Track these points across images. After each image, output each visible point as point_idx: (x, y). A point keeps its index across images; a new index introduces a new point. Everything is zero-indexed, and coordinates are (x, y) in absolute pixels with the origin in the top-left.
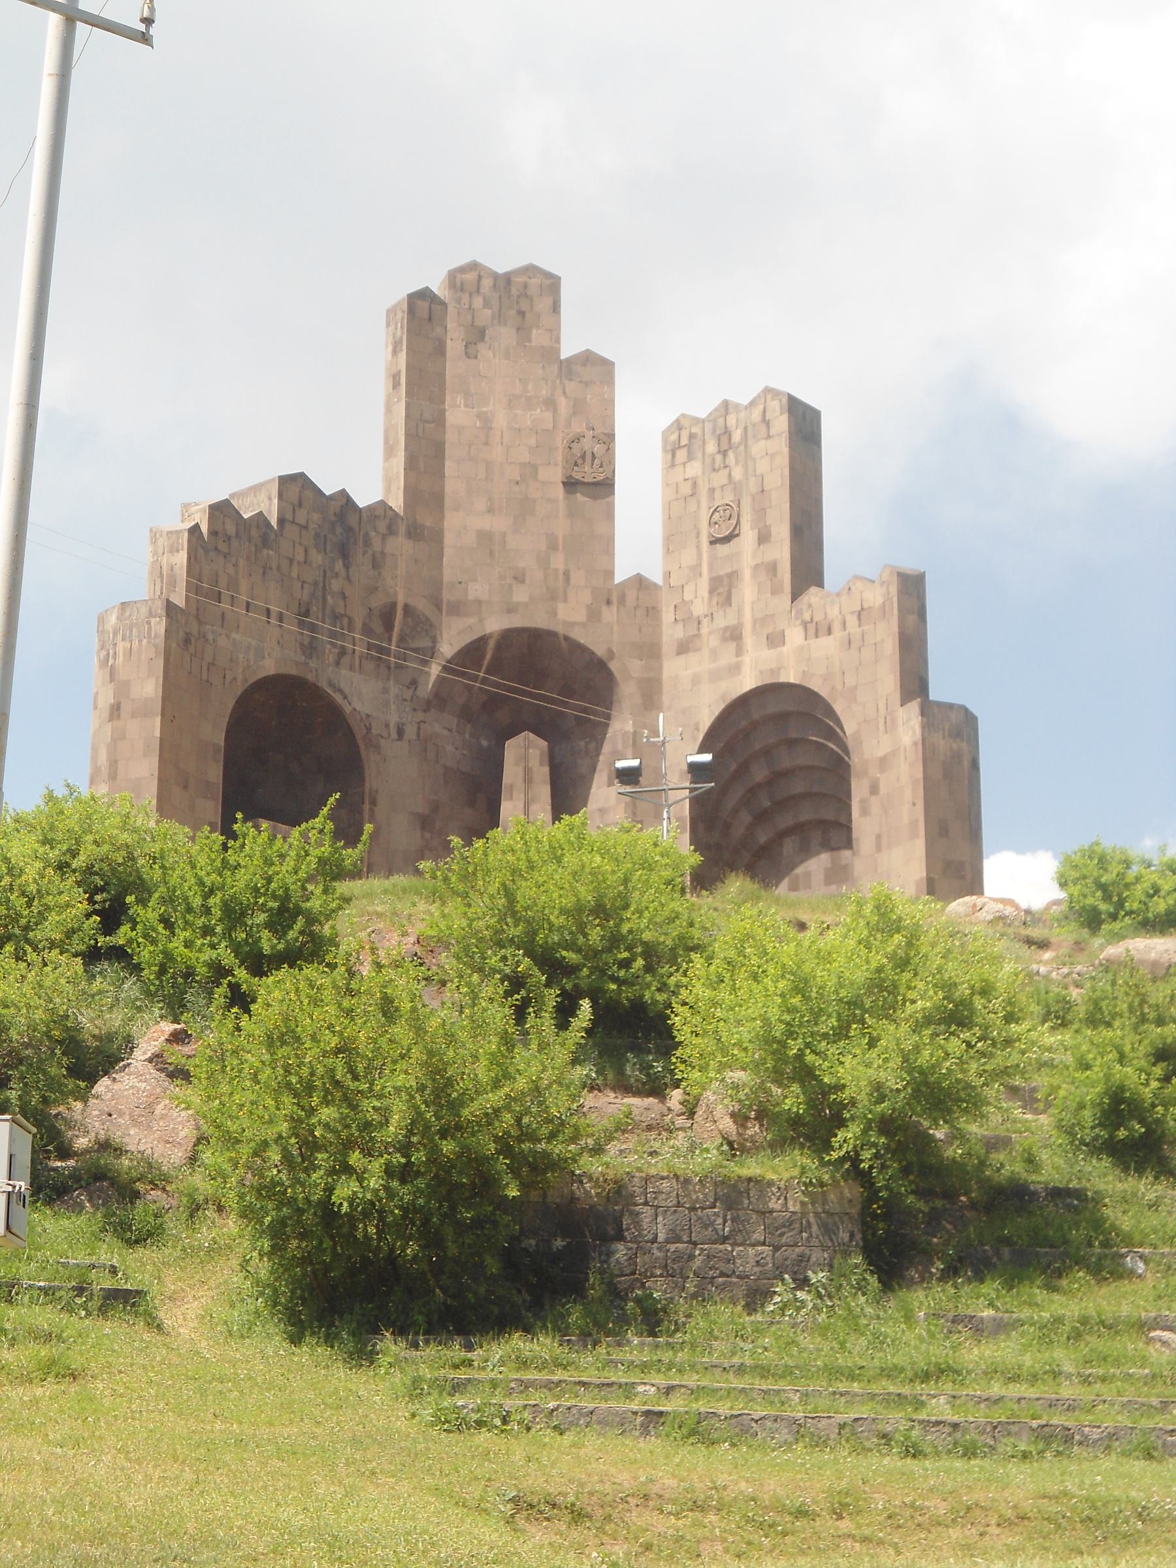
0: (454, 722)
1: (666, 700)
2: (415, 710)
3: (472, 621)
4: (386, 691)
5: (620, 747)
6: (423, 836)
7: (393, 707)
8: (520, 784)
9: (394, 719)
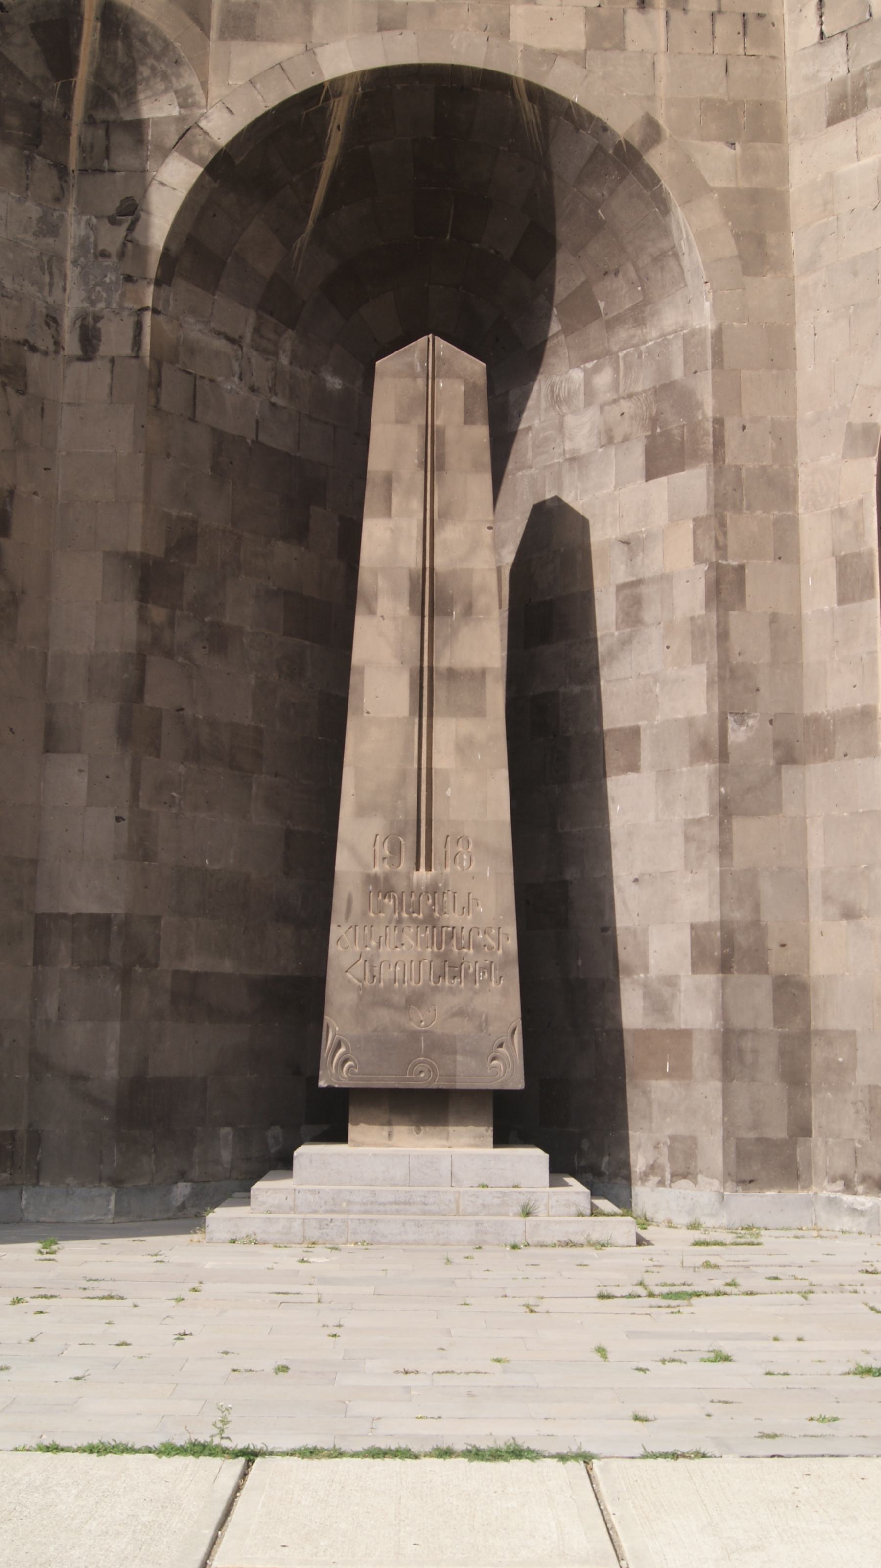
0: (245, 322)
1: (800, 245)
2: (129, 279)
3: (284, 51)
4: (50, 227)
5: (678, 373)
6: (143, 618)
7: (72, 273)
8: (410, 471)
9: (73, 303)
